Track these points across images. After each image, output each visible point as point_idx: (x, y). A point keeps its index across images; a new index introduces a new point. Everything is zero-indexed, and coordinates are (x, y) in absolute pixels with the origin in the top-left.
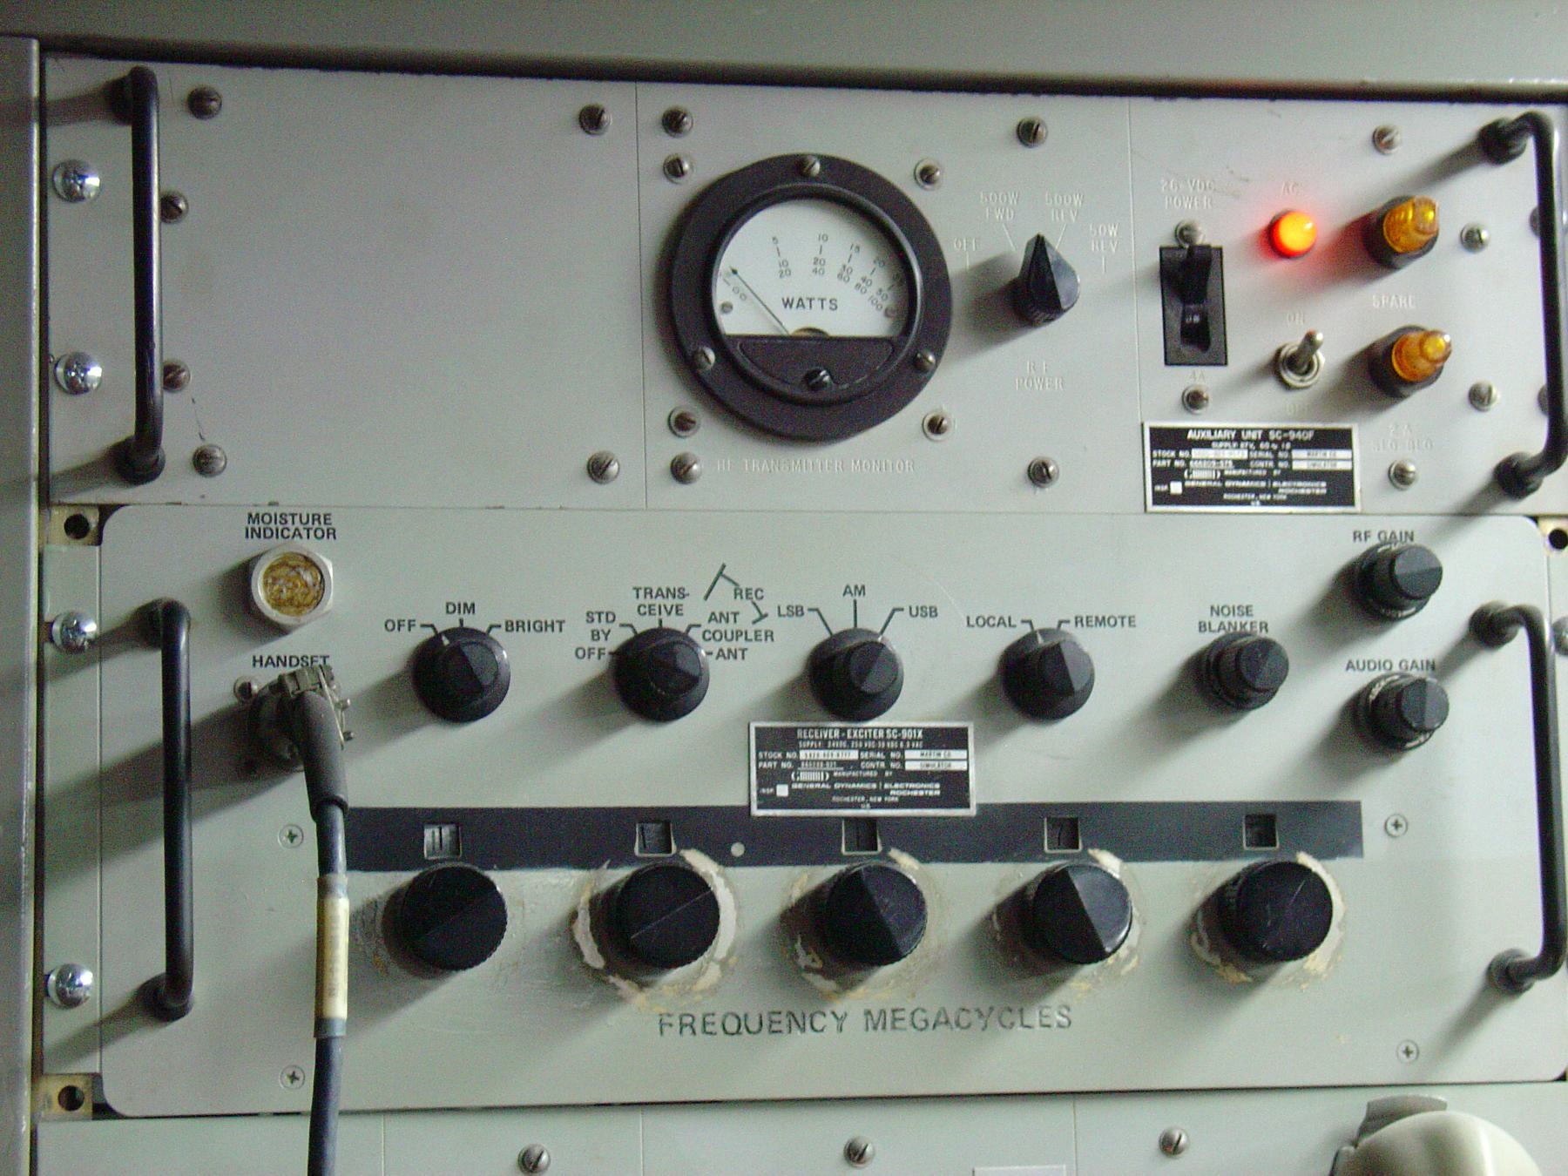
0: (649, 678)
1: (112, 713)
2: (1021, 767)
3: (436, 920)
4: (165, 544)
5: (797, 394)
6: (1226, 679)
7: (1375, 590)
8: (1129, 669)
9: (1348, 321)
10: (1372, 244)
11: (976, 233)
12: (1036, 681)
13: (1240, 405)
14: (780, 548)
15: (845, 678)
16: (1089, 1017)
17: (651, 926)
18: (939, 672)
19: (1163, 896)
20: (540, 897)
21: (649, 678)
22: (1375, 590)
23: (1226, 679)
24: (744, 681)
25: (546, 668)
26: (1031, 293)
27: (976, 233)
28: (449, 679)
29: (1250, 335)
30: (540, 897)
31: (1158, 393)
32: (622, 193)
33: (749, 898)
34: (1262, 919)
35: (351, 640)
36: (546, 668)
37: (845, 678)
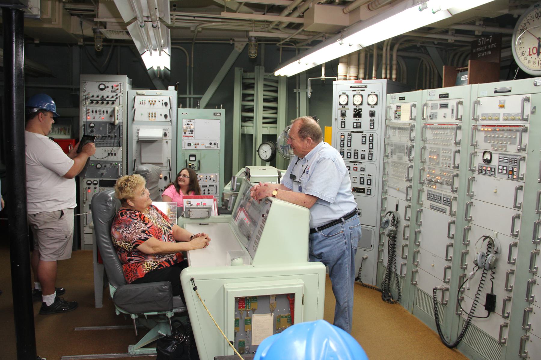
0: (98, 97)
1: (84, 97)
2: (107, 99)
3: (92, 102)
4: (86, 93)
5: (102, 89)
6: (113, 97)
7: (117, 95)
8: (110, 97)
9: (116, 88)
10: (117, 86)
11: (106, 86)
12: (108, 97)
13: (113, 90)
14: (102, 93)
15: (103, 97)
16: (109, 105)
17: (97, 103)
18: (105, 97)
19: (110, 102)
20: (95, 102)
21: (98, 97)
22: (117, 95)
23: (113, 97)
24: (100, 97)
25: (95, 96)
26: (108, 87)
27: (106, 86)
28: (93, 96)
29: (114, 88)
30: (95, 102)
31: (111, 89)
32: (98, 84)
33: (100, 102)
34: (113, 103)
35: (91, 95)
36: (95, 96)
37: (103, 97)
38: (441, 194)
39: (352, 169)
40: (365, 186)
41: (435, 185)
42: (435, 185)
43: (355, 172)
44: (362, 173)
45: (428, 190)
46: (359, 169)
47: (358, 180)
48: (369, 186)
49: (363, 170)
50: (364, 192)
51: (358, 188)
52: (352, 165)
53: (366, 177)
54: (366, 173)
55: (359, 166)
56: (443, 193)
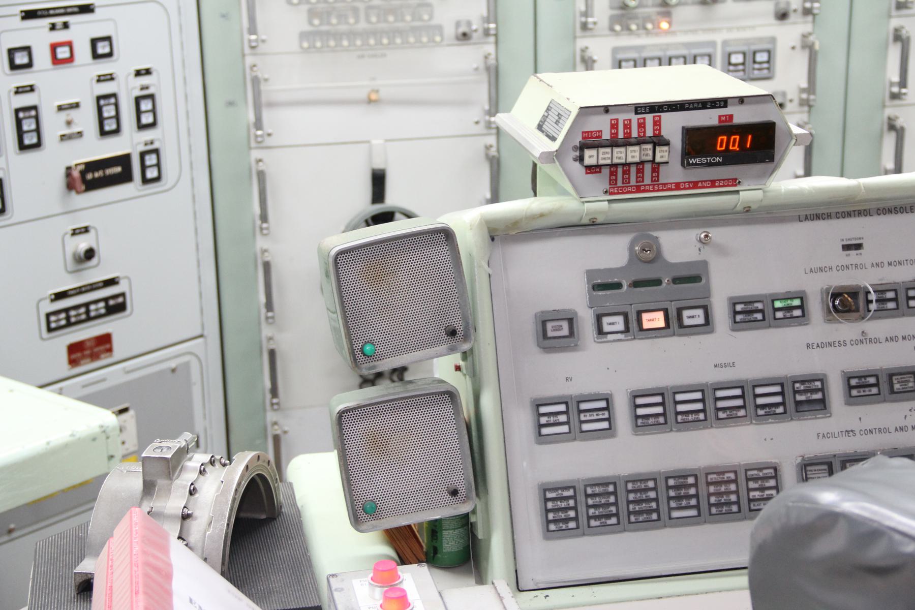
38: (713, 44)
39: (42, 57)
40: (130, 142)
41: (667, 15)
42: (667, 15)
43: (64, 72)
44: (104, 67)
45: (615, 50)
46: (83, 51)
47: (86, 120)
48: (148, 135)
49: (101, 48)
50: (125, 177)
51: (91, 166)
52: (38, 35)
53: (127, 89)
54: (122, 66)
55: (81, 31)
56: (719, 38)
